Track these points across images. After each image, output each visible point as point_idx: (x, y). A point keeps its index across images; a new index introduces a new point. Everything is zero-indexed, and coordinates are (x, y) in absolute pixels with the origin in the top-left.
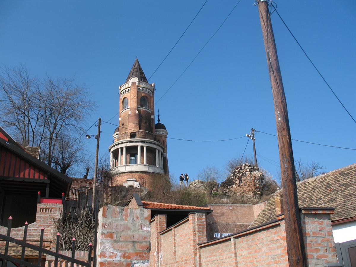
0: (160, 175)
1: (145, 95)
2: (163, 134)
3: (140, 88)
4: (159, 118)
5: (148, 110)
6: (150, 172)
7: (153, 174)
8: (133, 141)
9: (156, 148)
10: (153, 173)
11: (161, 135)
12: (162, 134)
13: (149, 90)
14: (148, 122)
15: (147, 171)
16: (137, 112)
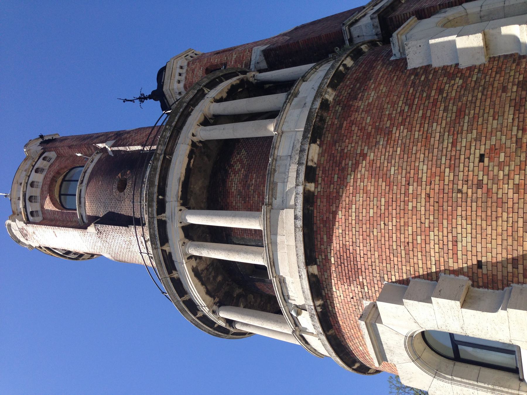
0: (325, 105)
1: (46, 187)
2: (183, 78)
3: (29, 210)
4: (150, 97)
5: (85, 172)
6: (309, 199)
7: (319, 173)
8: (172, 279)
9: (193, 144)
10: (310, 174)
11: (185, 87)
12: (182, 85)
13: (34, 171)
14: (120, 175)
15: (300, 223)
16: (91, 229)
